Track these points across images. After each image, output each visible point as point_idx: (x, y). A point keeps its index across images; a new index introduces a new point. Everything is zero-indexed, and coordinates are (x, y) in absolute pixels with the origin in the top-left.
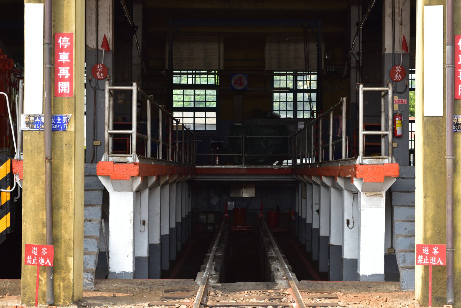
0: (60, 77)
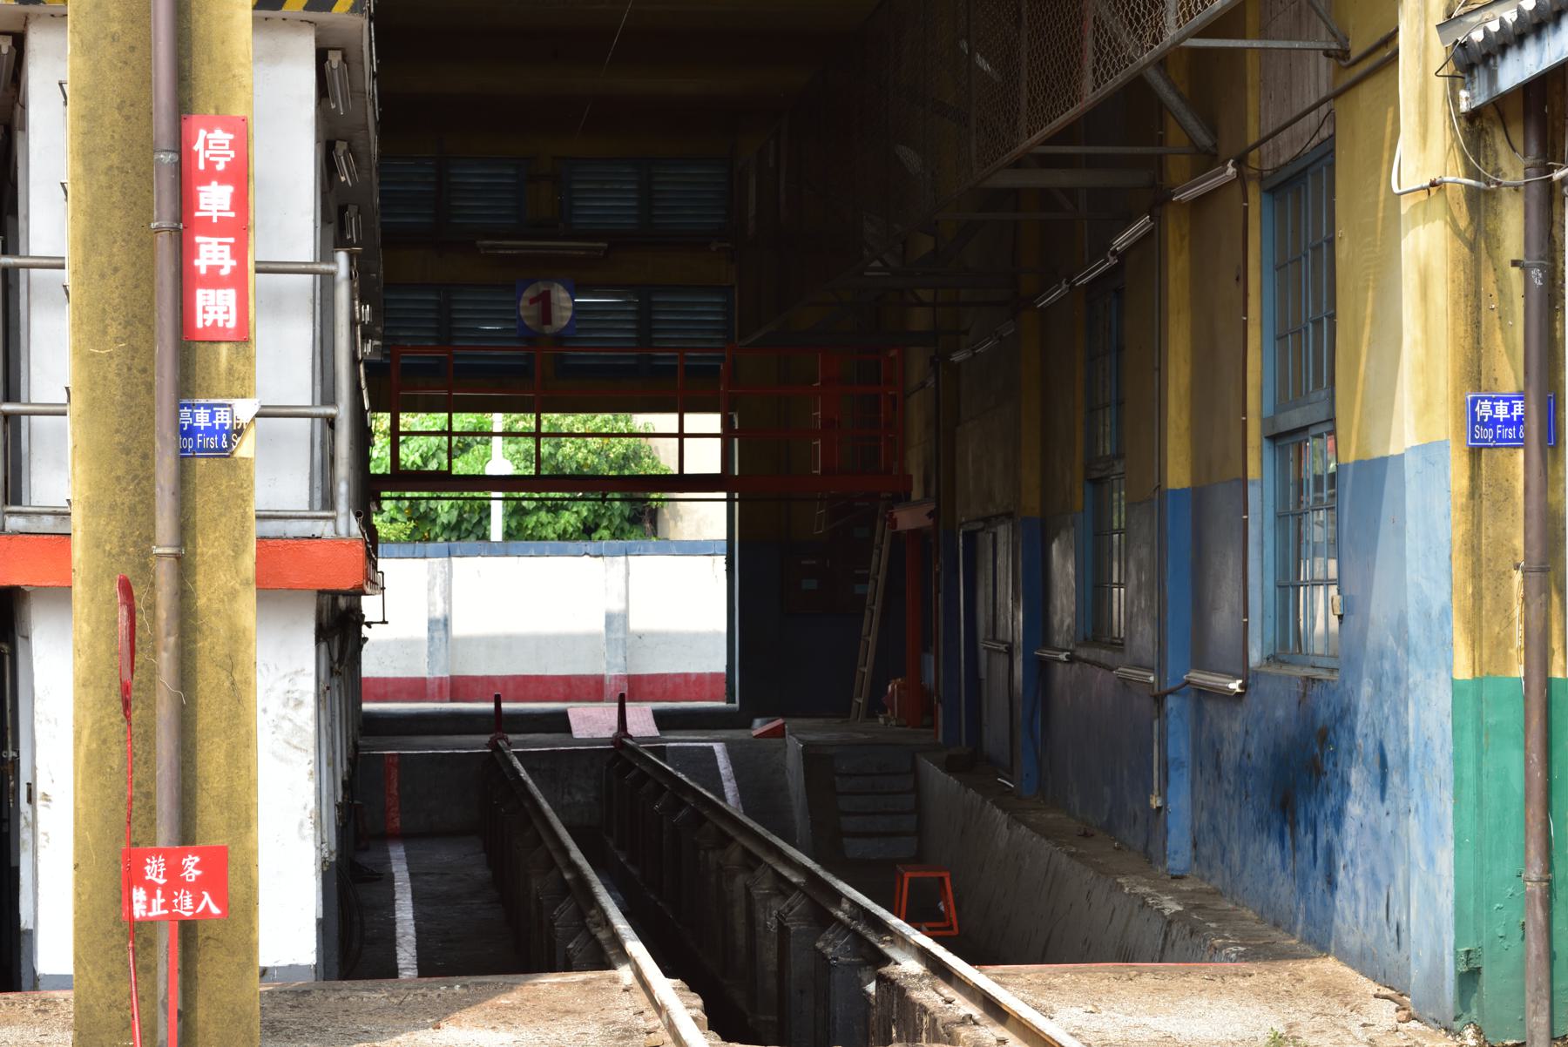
0: (203, 271)
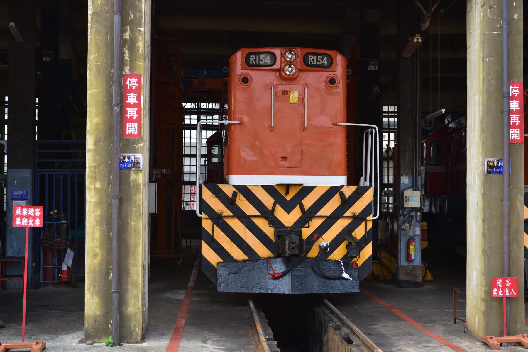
0: (128, 118)
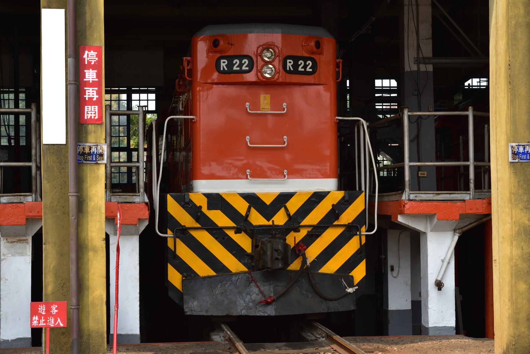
0: (87, 99)
